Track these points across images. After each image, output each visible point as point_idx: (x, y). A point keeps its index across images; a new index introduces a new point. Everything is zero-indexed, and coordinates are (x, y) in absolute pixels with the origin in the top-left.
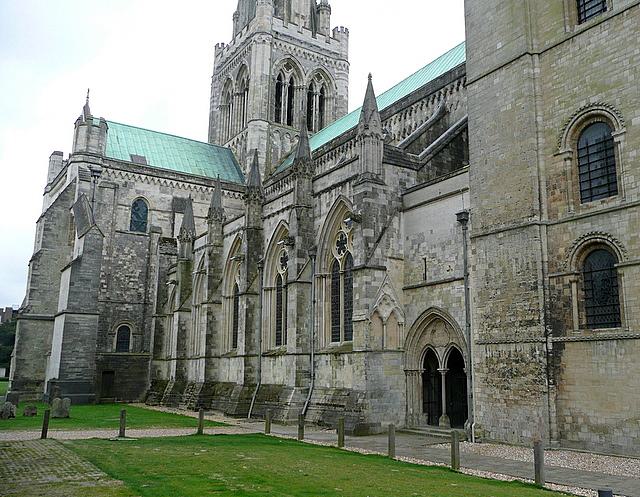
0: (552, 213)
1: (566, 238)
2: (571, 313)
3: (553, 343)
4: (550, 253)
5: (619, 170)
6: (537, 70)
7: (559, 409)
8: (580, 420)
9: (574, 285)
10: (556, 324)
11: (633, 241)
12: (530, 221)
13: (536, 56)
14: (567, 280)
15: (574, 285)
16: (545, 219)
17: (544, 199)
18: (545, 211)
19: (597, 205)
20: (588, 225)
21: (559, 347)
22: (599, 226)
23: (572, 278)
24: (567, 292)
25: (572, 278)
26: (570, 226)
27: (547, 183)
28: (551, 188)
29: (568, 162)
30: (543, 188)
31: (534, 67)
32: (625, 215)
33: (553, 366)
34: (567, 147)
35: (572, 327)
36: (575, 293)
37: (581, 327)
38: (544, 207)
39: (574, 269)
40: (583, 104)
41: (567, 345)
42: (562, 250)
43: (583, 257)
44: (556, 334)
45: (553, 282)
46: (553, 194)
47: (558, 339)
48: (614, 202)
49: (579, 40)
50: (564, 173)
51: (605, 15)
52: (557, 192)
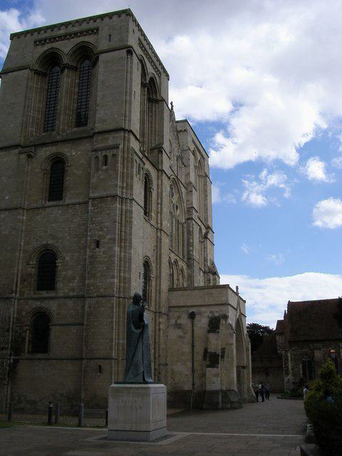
0: (22, 293)
1: (27, 307)
2: (24, 345)
3: (14, 360)
4: (18, 313)
5: (57, 279)
6: (25, 218)
7: (12, 393)
8: (23, 398)
9: (28, 332)
10: (17, 350)
11: (58, 314)
12: (10, 296)
13: (25, 211)
14: (25, 328)
15: (28, 332)
16: (18, 296)
17: (19, 284)
18: (18, 292)
19: (44, 294)
20: (39, 303)
21: (16, 362)
22: (44, 305)
23: (28, 327)
24: (24, 334)
25: (28, 327)
26: (30, 302)
27: (21, 278)
28: (23, 280)
29: (34, 269)
30: (19, 281)
31: (23, 216)
32: (57, 301)
33: (13, 370)
34: (33, 262)
35: (24, 352)
36: (28, 335)
37: (28, 352)
38: (18, 289)
39: (29, 323)
40: (44, 242)
41: (21, 361)
42: (24, 313)
43: (34, 318)
44: (17, 355)
45: (18, 328)
46: (23, 284)
47: (16, 358)
48: (52, 294)
49: (48, 210)
50: (31, 274)
51: (61, 203)
52: (26, 283)
